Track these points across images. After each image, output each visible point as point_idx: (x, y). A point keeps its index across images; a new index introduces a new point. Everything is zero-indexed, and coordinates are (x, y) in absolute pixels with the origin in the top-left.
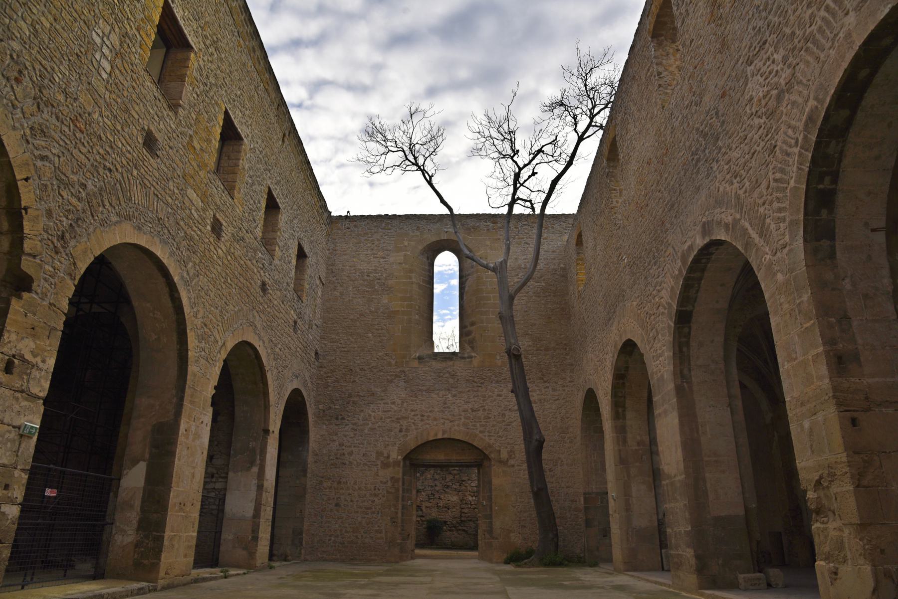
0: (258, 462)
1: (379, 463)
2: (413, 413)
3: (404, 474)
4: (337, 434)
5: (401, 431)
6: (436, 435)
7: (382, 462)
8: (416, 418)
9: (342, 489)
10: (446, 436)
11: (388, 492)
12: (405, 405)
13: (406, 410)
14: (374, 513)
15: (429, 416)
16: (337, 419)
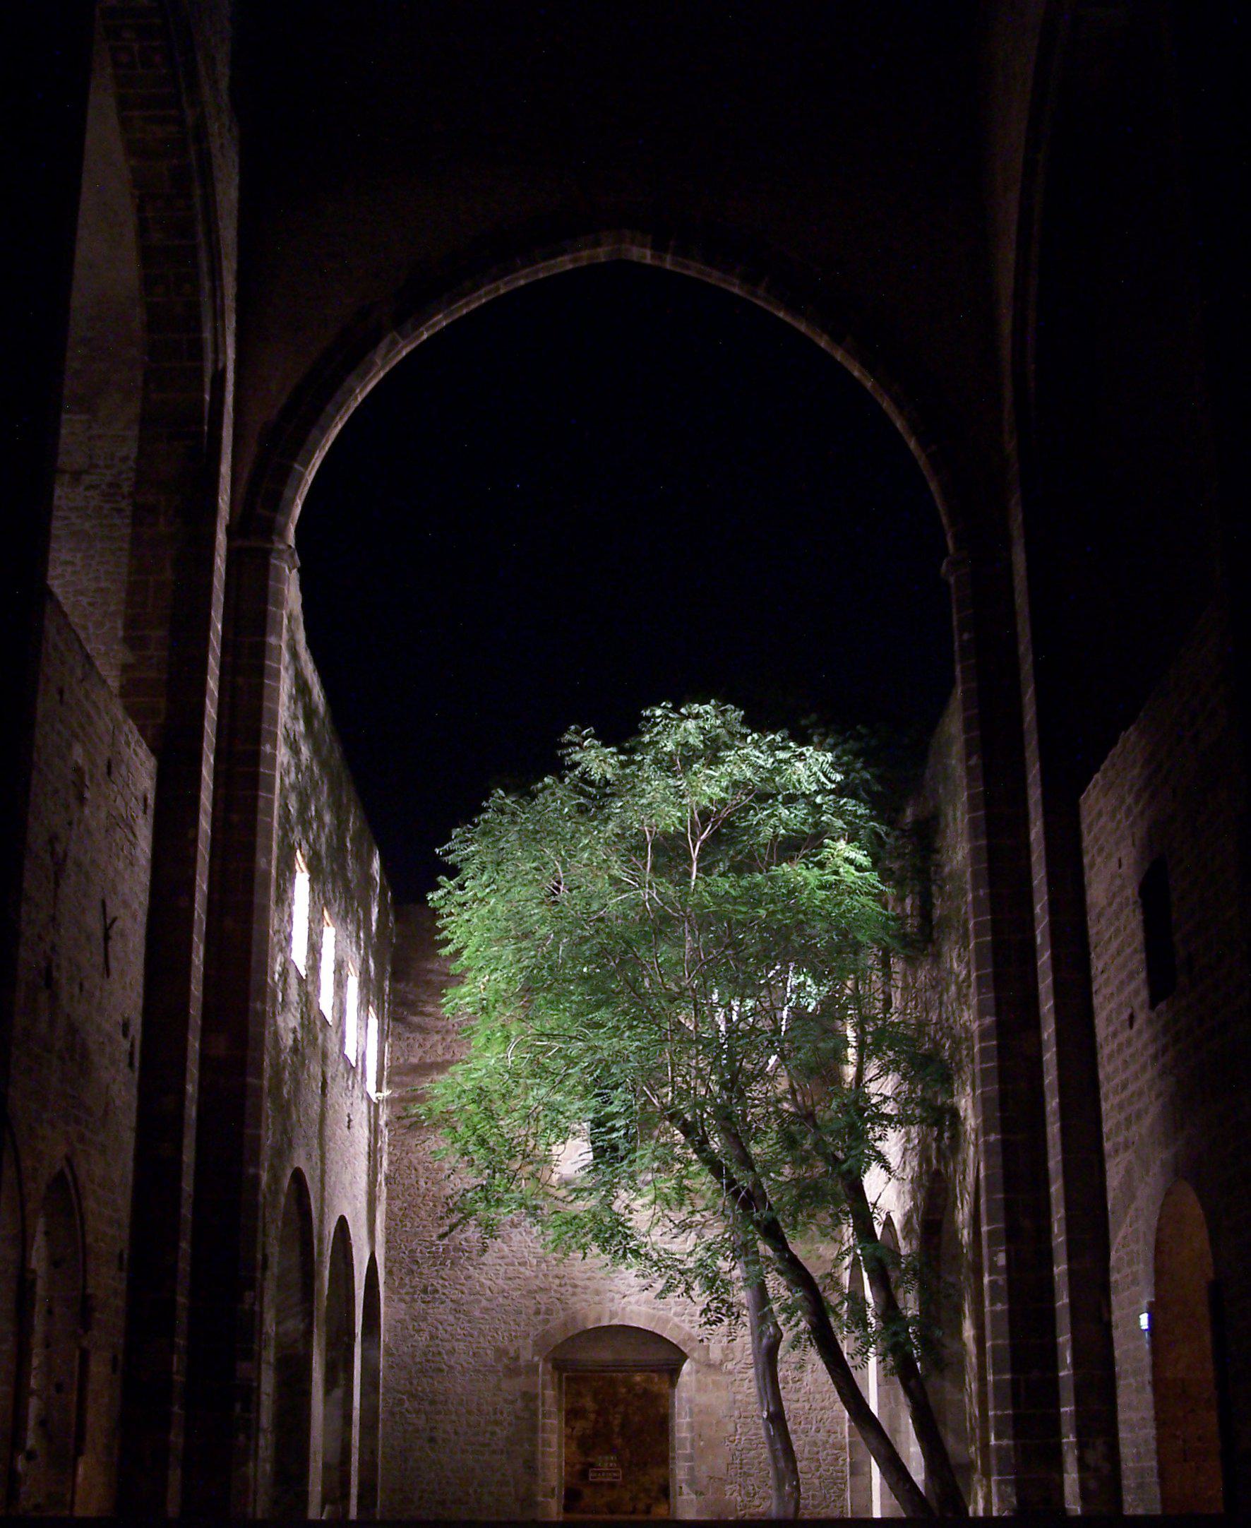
0: (342, 1382)
1: (500, 1367)
2: (557, 1281)
3: (544, 1387)
4: (425, 1319)
5: (537, 1312)
6: (599, 1319)
7: (507, 1366)
8: (563, 1290)
9: (439, 1413)
10: (615, 1322)
11: (518, 1418)
12: (544, 1266)
13: (545, 1275)
14: (494, 1452)
15: (586, 1288)
16: (425, 1291)
